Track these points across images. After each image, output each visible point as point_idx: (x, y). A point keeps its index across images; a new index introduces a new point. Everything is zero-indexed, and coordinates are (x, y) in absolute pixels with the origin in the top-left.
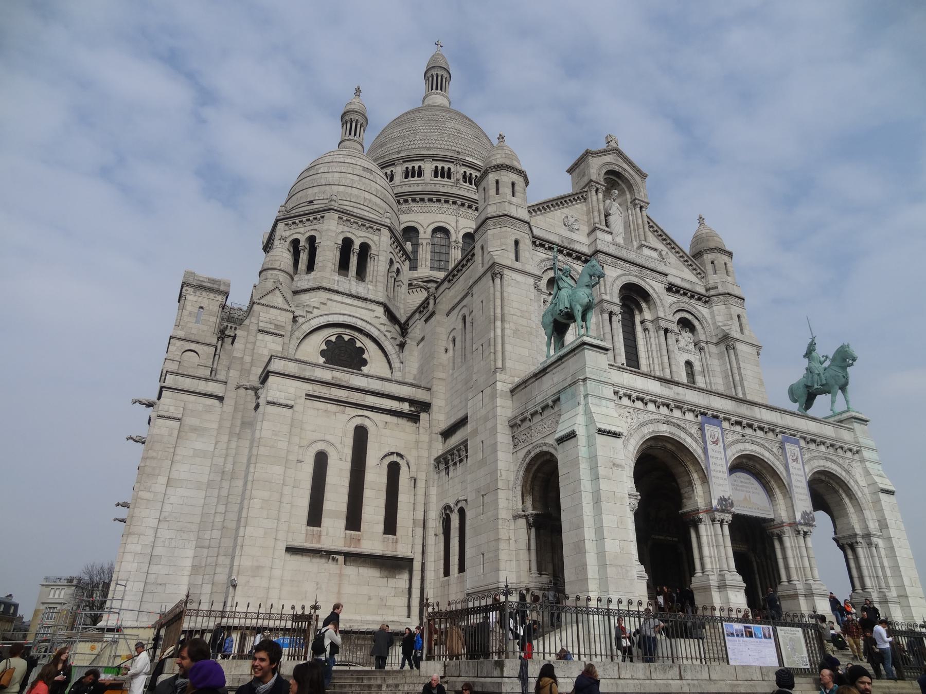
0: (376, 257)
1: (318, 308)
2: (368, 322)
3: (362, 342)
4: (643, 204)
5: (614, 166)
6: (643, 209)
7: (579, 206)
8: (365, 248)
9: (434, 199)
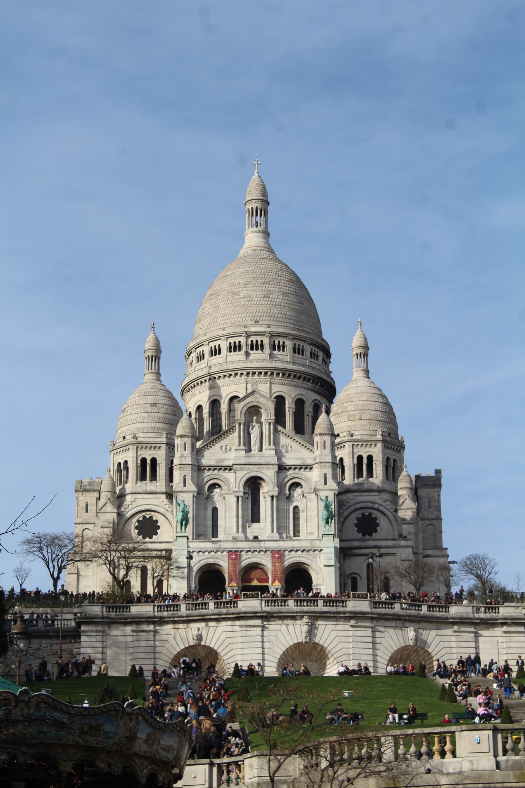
0: (160, 465)
1: (132, 504)
2: (157, 506)
3: (156, 516)
4: (270, 421)
5: (252, 403)
6: (272, 424)
7: (230, 436)
8: (154, 461)
9: (228, 375)
